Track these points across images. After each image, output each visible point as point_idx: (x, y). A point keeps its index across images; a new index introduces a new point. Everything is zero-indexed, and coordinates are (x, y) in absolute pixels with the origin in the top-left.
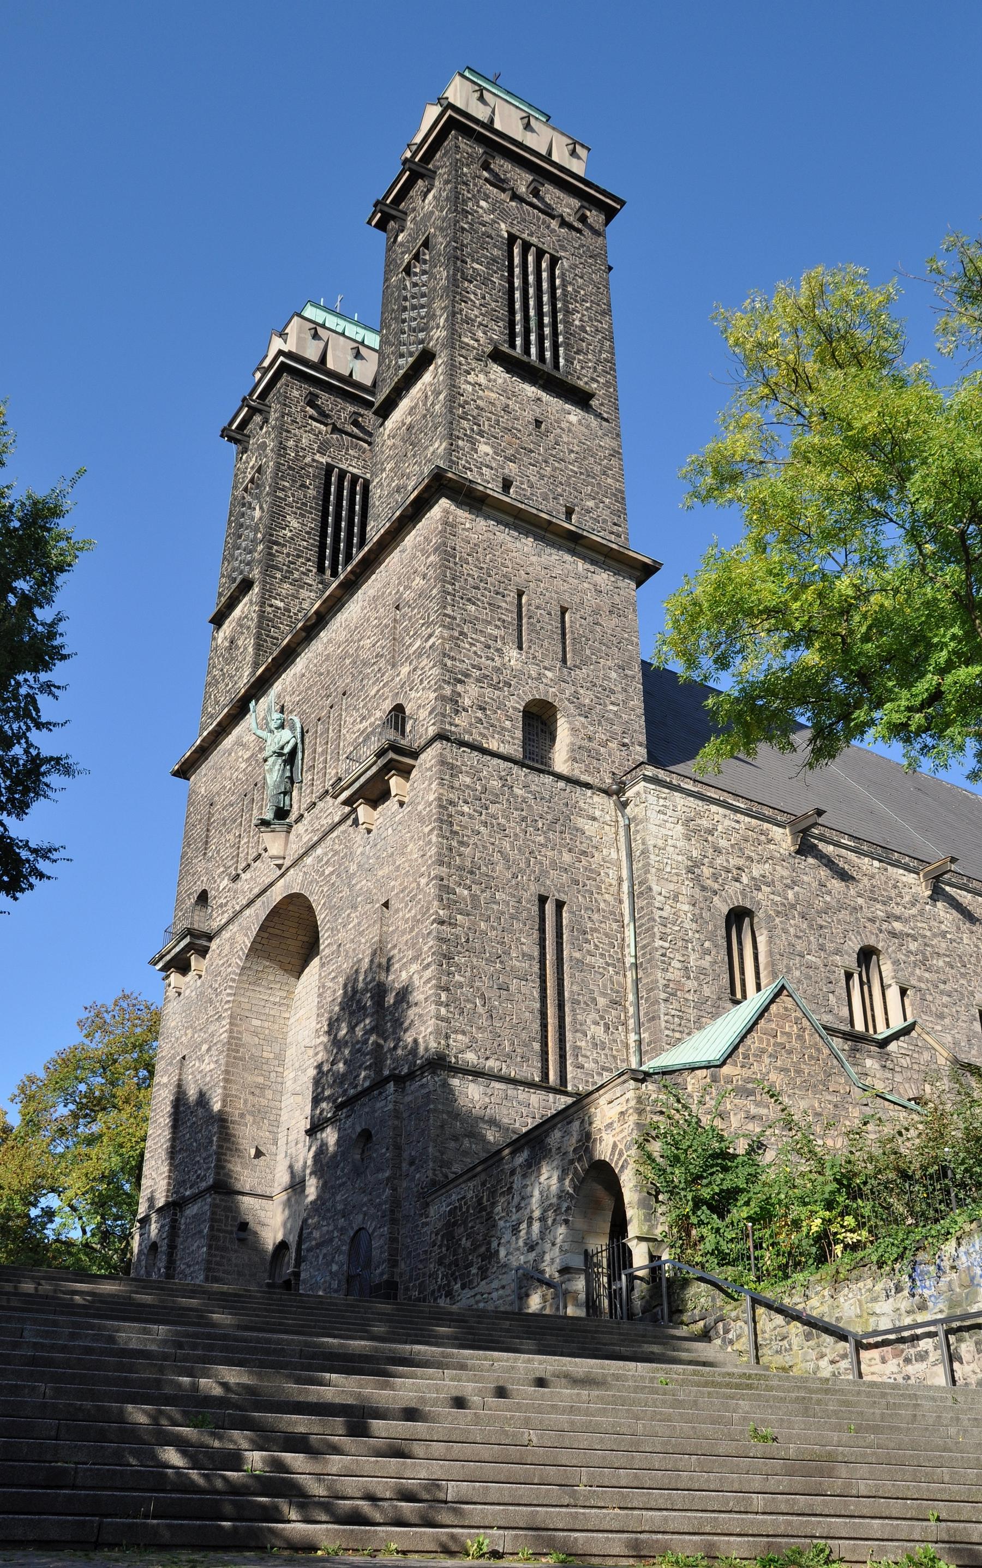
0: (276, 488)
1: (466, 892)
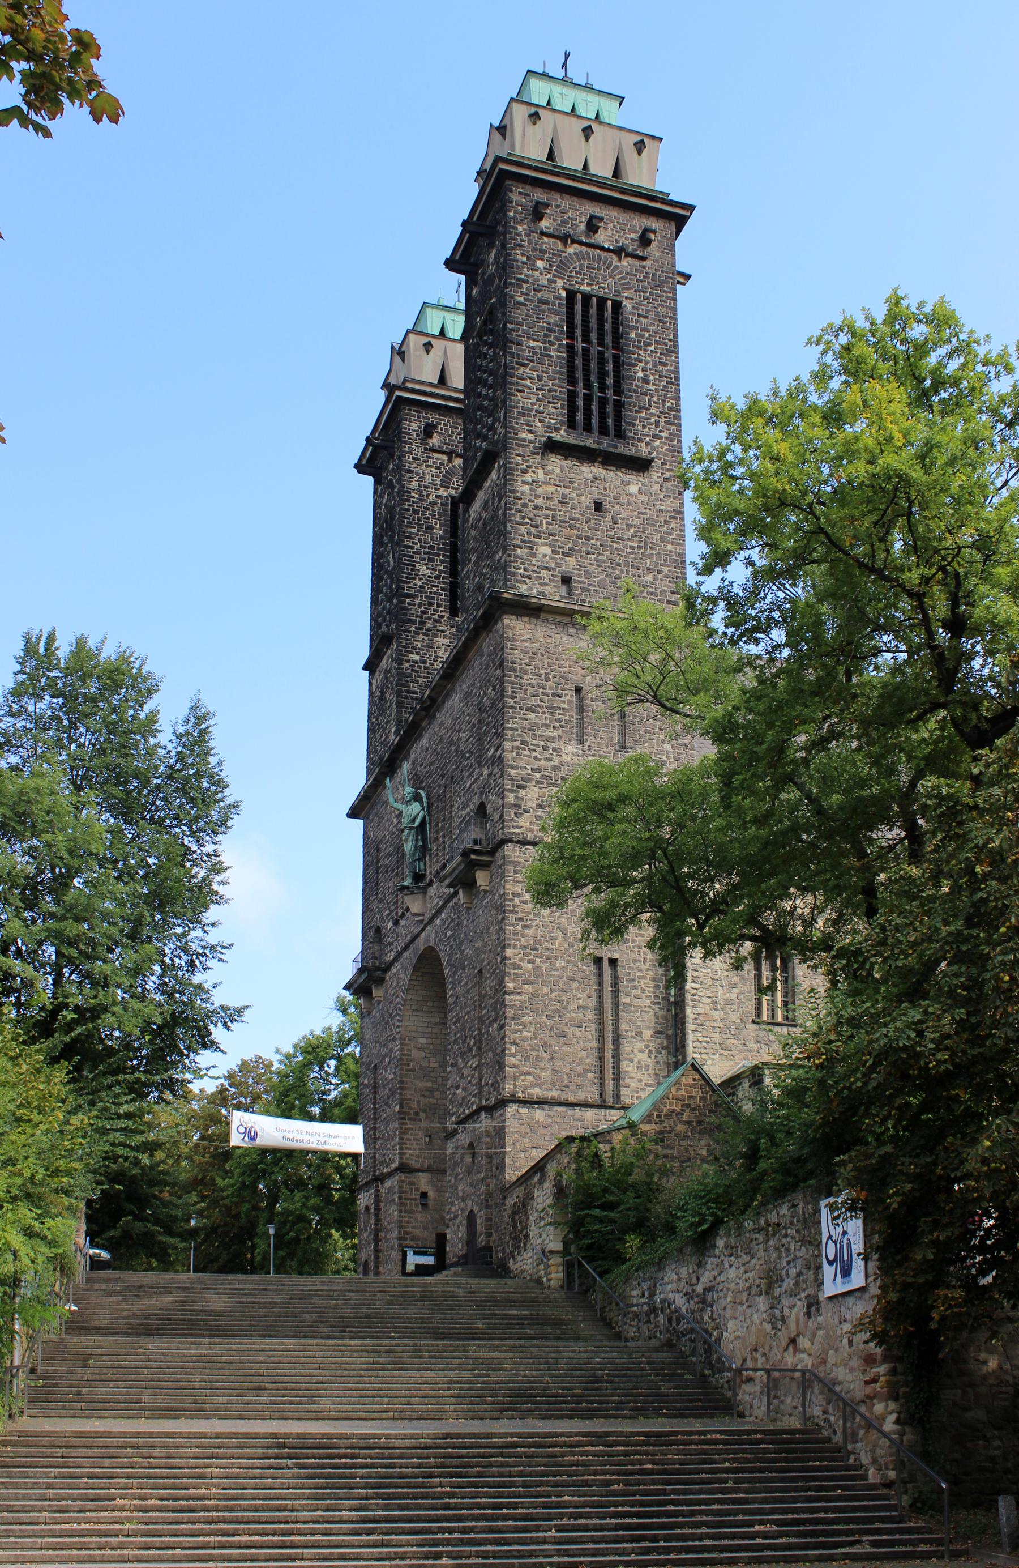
1: (530, 966)
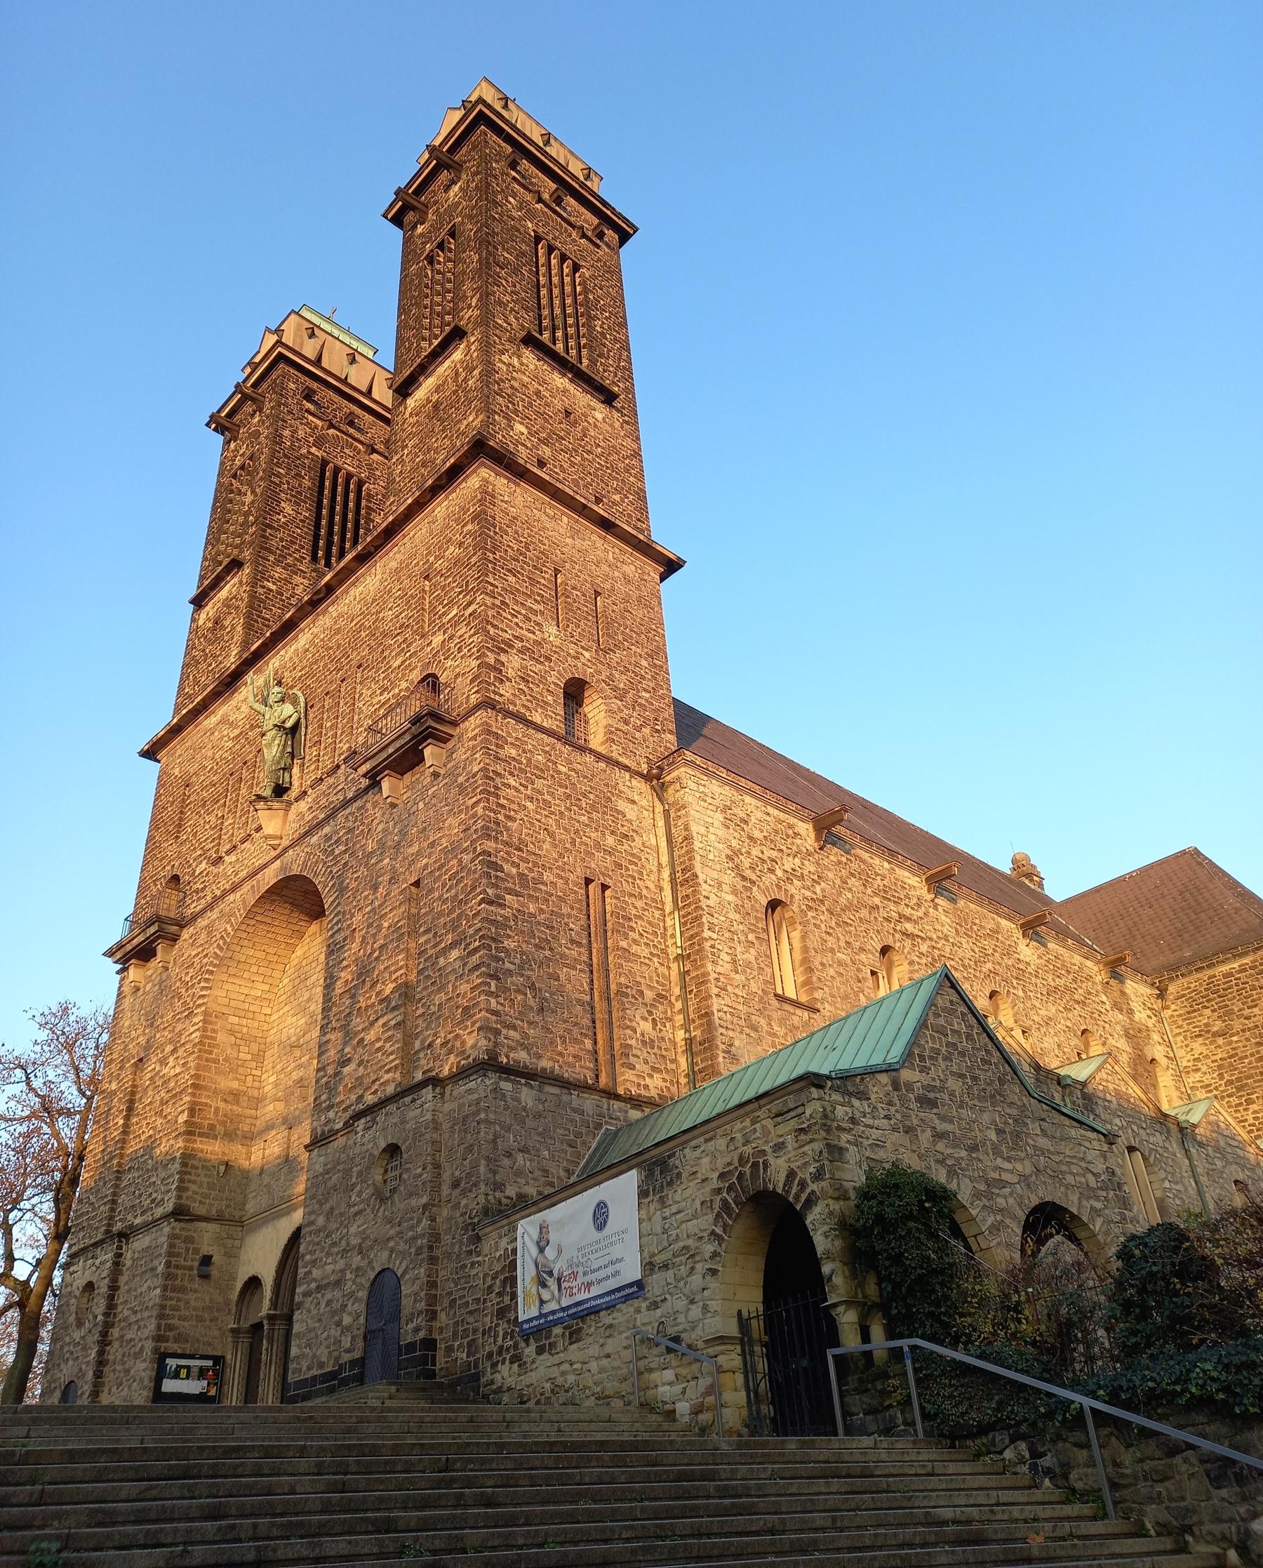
0: (270, 473)
1: (514, 871)
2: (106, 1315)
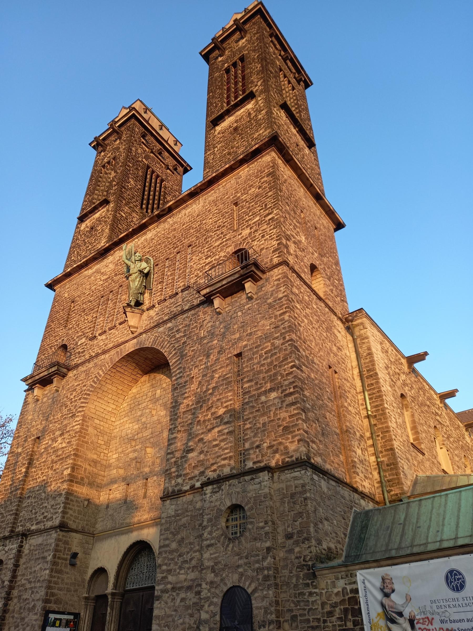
0: (125, 164)
2: (11, 581)
